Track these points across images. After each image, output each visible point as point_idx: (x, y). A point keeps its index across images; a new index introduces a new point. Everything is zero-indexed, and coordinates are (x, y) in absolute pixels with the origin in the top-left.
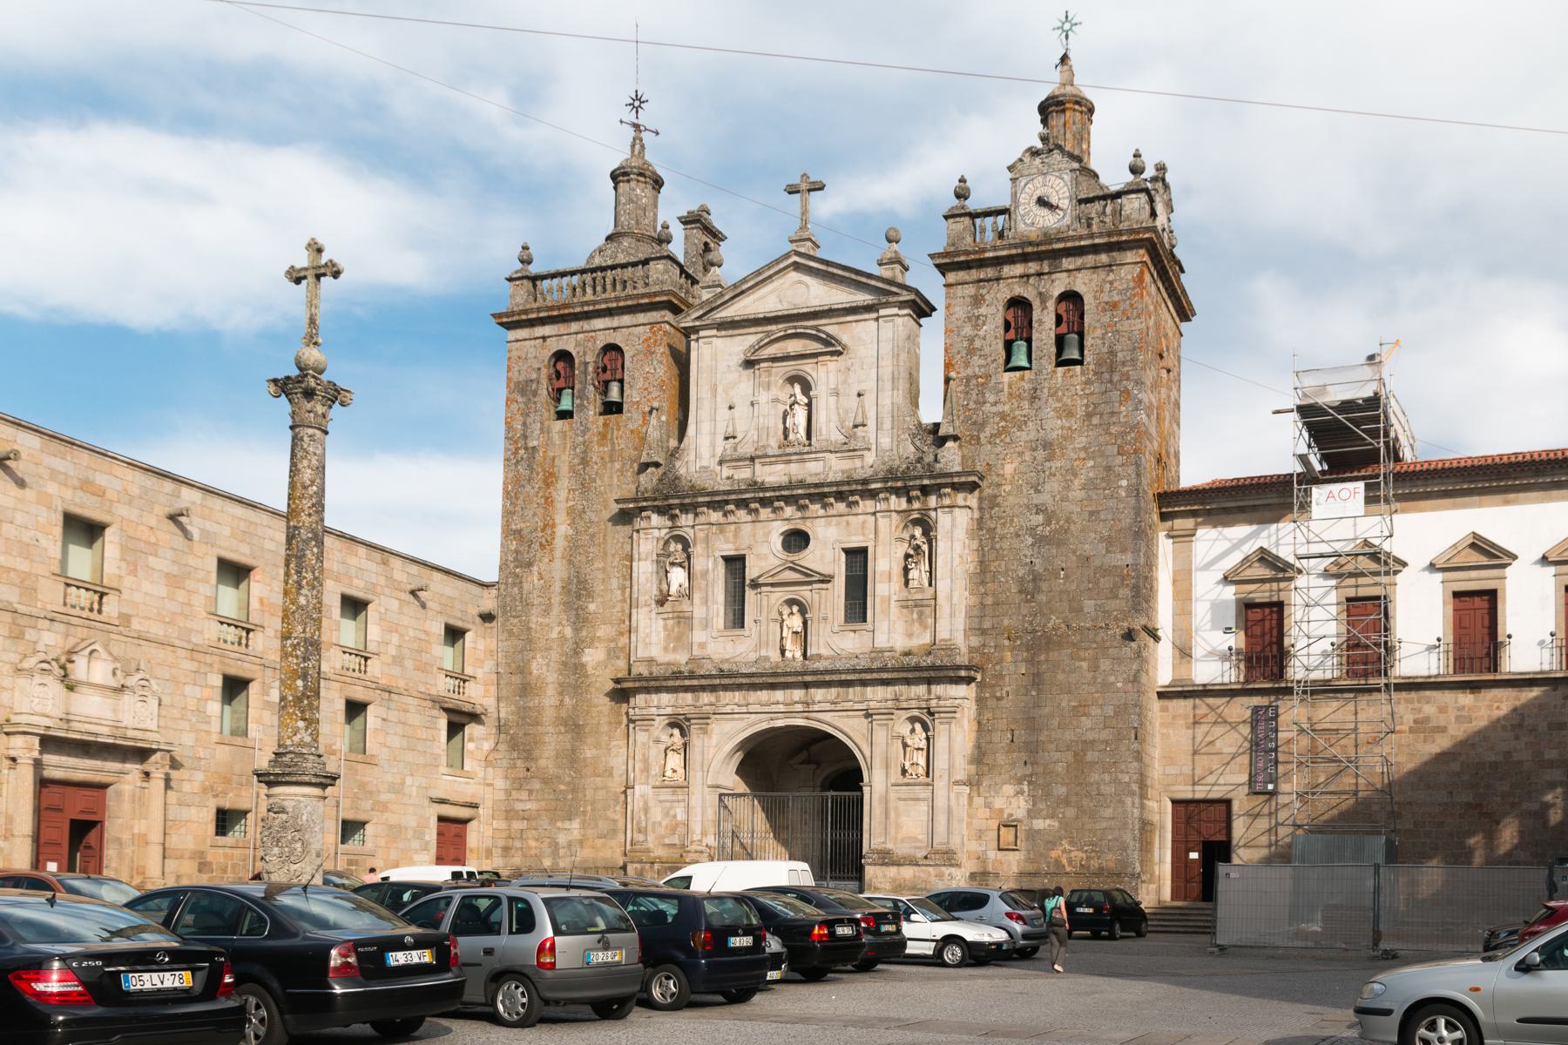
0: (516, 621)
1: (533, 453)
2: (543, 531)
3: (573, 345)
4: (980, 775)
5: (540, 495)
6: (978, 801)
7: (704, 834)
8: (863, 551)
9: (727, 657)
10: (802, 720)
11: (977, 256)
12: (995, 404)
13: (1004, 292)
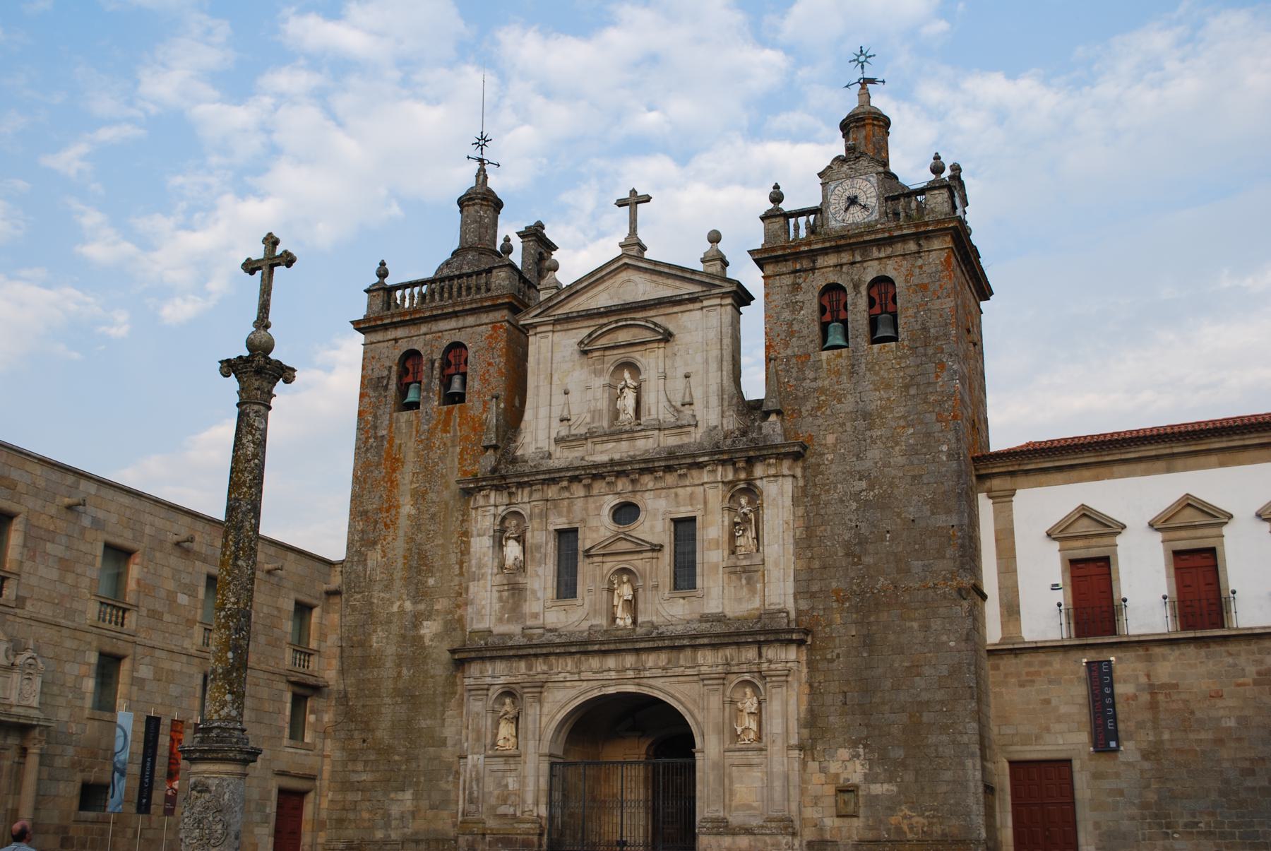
0: (359, 596)
1: (382, 441)
2: (388, 511)
3: (422, 345)
4: (814, 740)
5: (386, 479)
6: (813, 766)
7: (537, 804)
8: (693, 519)
9: (560, 626)
10: (633, 687)
11: (793, 251)
12: (815, 379)
13: (820, 281)
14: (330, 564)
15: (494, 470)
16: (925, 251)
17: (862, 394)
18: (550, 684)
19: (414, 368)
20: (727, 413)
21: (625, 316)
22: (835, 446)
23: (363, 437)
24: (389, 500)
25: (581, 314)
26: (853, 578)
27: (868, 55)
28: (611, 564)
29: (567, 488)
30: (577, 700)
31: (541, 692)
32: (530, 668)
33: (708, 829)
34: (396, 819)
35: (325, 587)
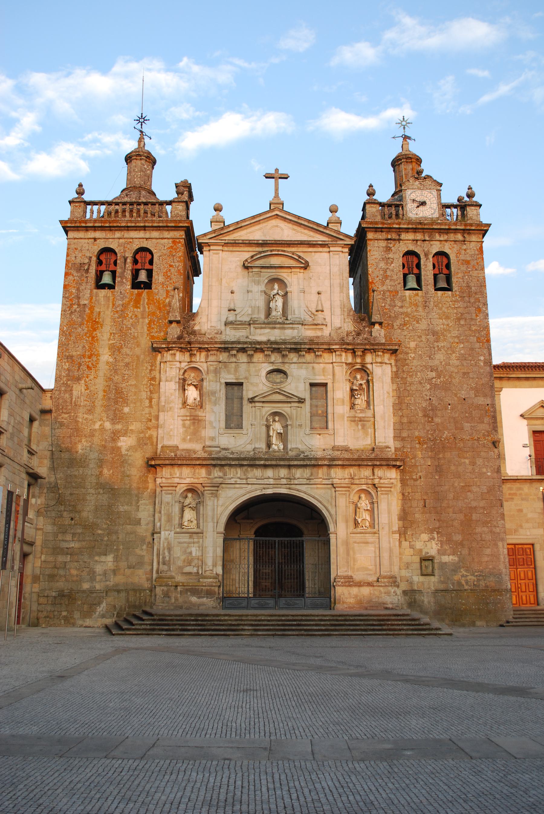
0: (66, 416)
2: (90, 357)
3: (117, 245)
4: (406, 528)
5: (88, 335)
7: (215, 565)
8: (325, 385)
9: (230, 447)
10: (285, 490)
11: (389, 226)
12: (402, 307)
13: (404, 247)
14: (43, 391)
15: (180, 338)
16: (468, 241)
17: (432, 320)
18: (223, 485)
19: (106, 262)
20: (347, 320)
21: (272, 249)
22: (415, 349)
23: (68, 304)
24: (90, 349)
25: (245, 242)
26: (428, 431)
27: (408, 122)
28: (268, 409)
29: (235, 355)
30: (244, 497)
31: (217, 491)
32: (209, 473)
33: (342, 583)
34: (100, 575)
35: (40, 407)
